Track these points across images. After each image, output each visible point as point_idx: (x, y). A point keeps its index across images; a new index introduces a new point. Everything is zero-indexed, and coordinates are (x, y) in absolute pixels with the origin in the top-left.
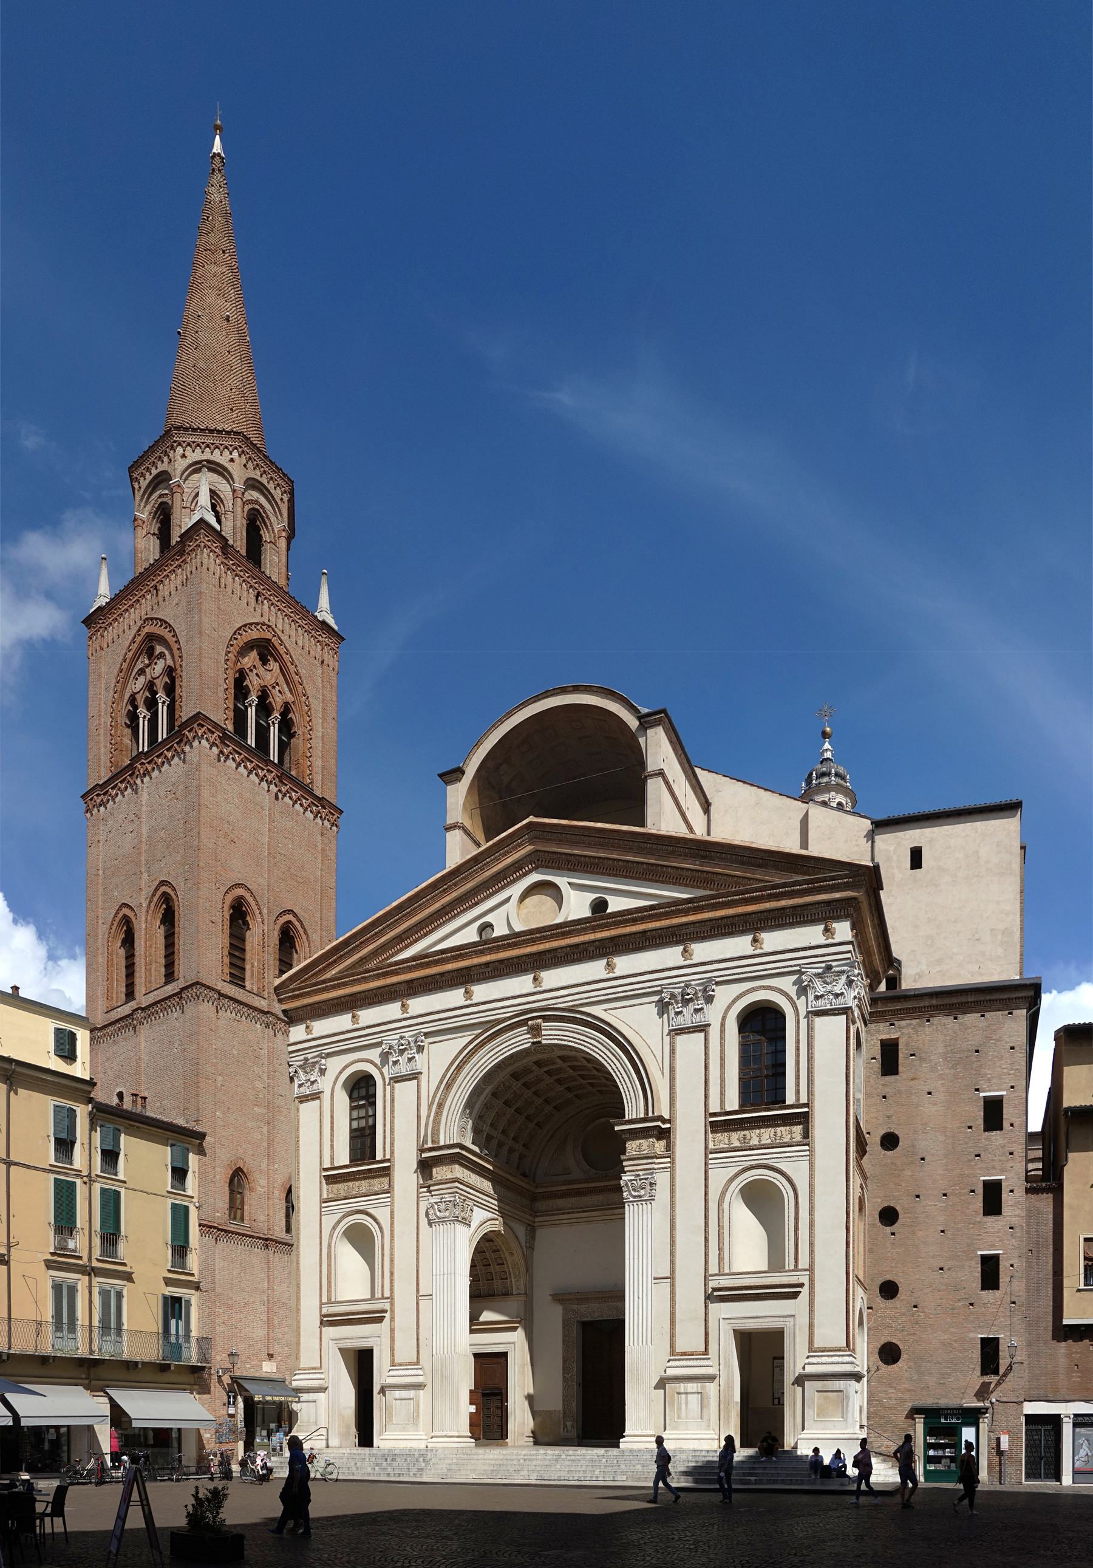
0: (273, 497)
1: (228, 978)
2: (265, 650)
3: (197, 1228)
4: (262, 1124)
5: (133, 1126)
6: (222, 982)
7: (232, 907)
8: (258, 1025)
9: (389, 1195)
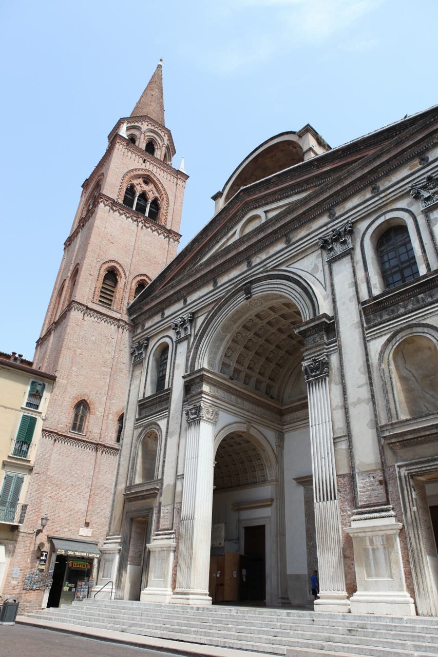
1: (98, 302)
2: (147, 180)
5: (5, 368)
7: (108, 271)
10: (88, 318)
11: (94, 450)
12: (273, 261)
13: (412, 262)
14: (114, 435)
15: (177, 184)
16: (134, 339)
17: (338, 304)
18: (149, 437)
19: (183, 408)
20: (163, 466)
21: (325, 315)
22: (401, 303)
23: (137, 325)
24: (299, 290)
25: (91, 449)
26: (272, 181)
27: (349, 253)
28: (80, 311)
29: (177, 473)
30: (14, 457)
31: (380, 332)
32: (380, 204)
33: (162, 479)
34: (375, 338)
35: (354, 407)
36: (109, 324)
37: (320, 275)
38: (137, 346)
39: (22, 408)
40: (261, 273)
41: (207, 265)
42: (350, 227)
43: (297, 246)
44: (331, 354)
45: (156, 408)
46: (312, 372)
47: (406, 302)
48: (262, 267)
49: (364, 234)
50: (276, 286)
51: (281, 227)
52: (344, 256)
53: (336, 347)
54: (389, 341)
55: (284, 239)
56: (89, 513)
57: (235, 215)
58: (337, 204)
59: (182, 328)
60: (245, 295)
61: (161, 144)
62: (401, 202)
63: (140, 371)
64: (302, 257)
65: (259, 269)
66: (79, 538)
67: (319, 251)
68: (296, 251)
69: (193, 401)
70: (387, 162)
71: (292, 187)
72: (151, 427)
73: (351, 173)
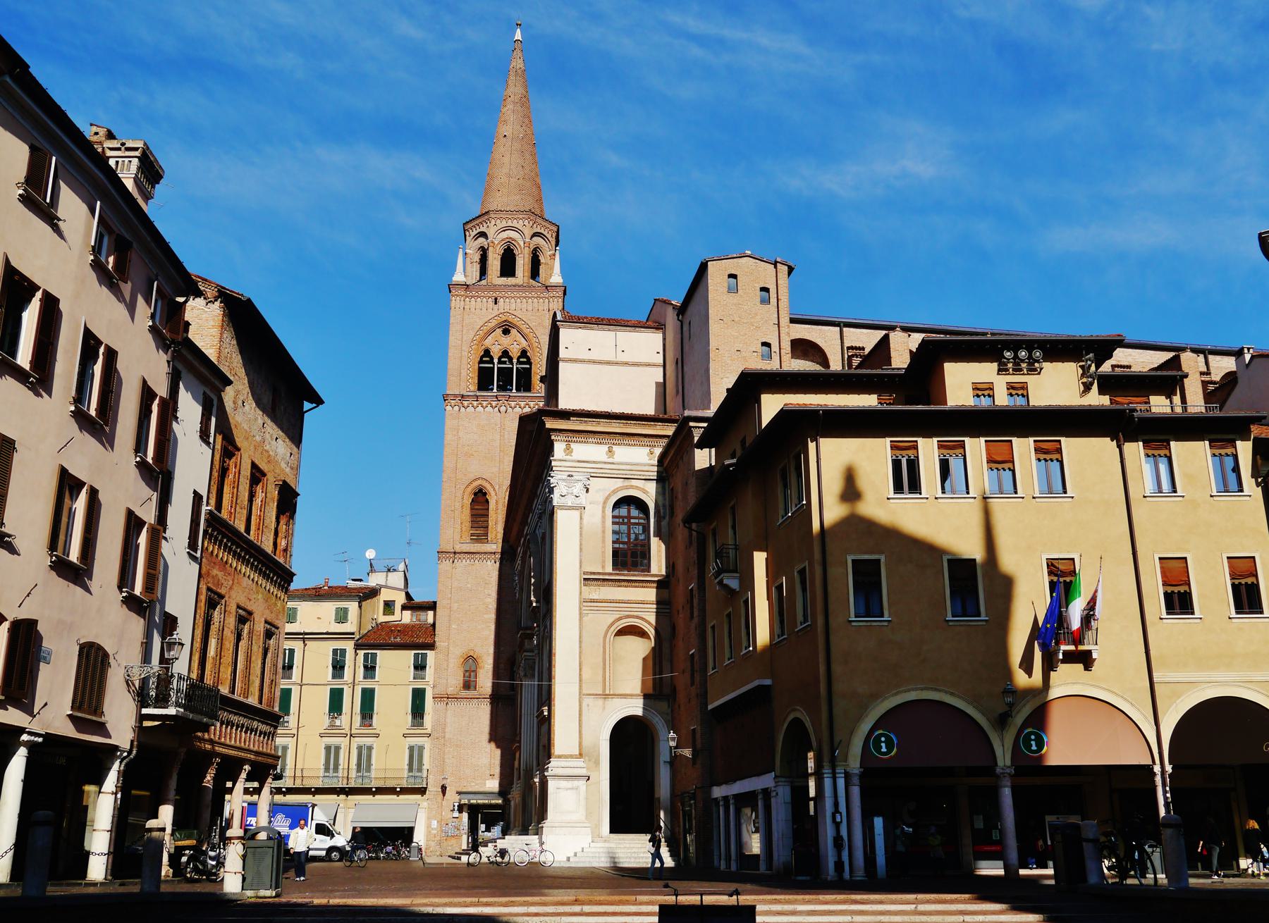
3: (432, 700)
36: (485, 561)
61: (522, 243)
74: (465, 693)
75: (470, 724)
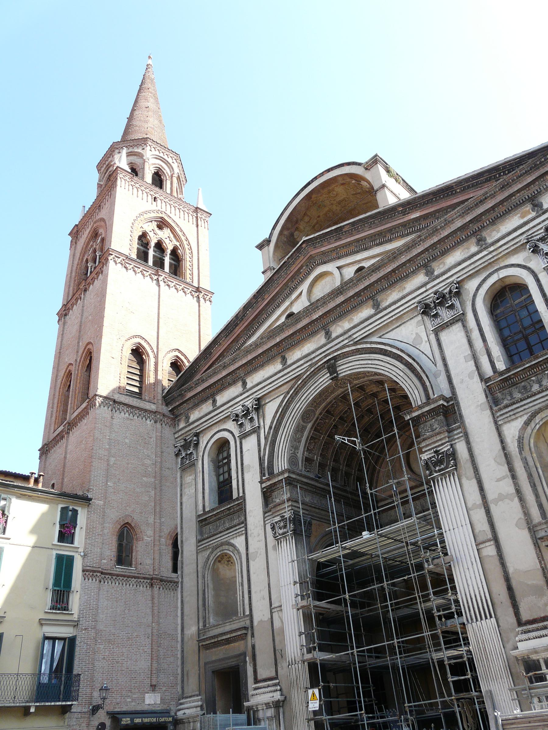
0: (167, 162)
2: (162, 224)
4: (150, 489)
6: (119, 395)
8: (148, 422)
9: (243, 525)
10: (117, 414)
11: (148, 587)
12: (360, 330)
13: (537, 326)
14: (169, 564)
15: (197, 226)
16: (176, 436)
17: (455, 381)
18: (219, 561)
19: (264, 522)
20: (250, 598)
21: (443, 397)
22: (533, 378)
23: (176, 417)
24: (402, 366)
25: (145, 586)
26: (344, 230)
27: (461, 319)
28: (106, 408)
29: (271, 605)
30: (52, 613)
31: (514, 414)
32: (490, 259)
33: (251, 615)
34: (509, 421)
35: (496, 505)
37: (425, 347)
38: (182, 444)
39: (53, 545)
40: (348, 346)
41: (271, 337)
42: (457, 288)
43: (390, 312)
44: (456, 443)
45: (224, 523)
46: (435, 464)
47: (540, 377)
48: (346, 339)
49: (475, 296)
50: (370, 362)
51: (365, 288)
52: (454, 323)
53: (461, 435)
54: (527, 423)
55: (371, 303)
56: (154, 672)
57: (298, 271)
58: (435, 259)
59: (246, 418)
60: (328, 375)
62: (516, 256)
63: (193, 477)
64: (398, 325)
65: (343, 341)
66: (146, 708)
67: (419, 318)
68: (390, 318)
69: (278, 511)
70: (493, 208)
71: (372, 238)
72: (221, 548)
73: (448, 223)
74: (119, 569)
75: (127, 611)
